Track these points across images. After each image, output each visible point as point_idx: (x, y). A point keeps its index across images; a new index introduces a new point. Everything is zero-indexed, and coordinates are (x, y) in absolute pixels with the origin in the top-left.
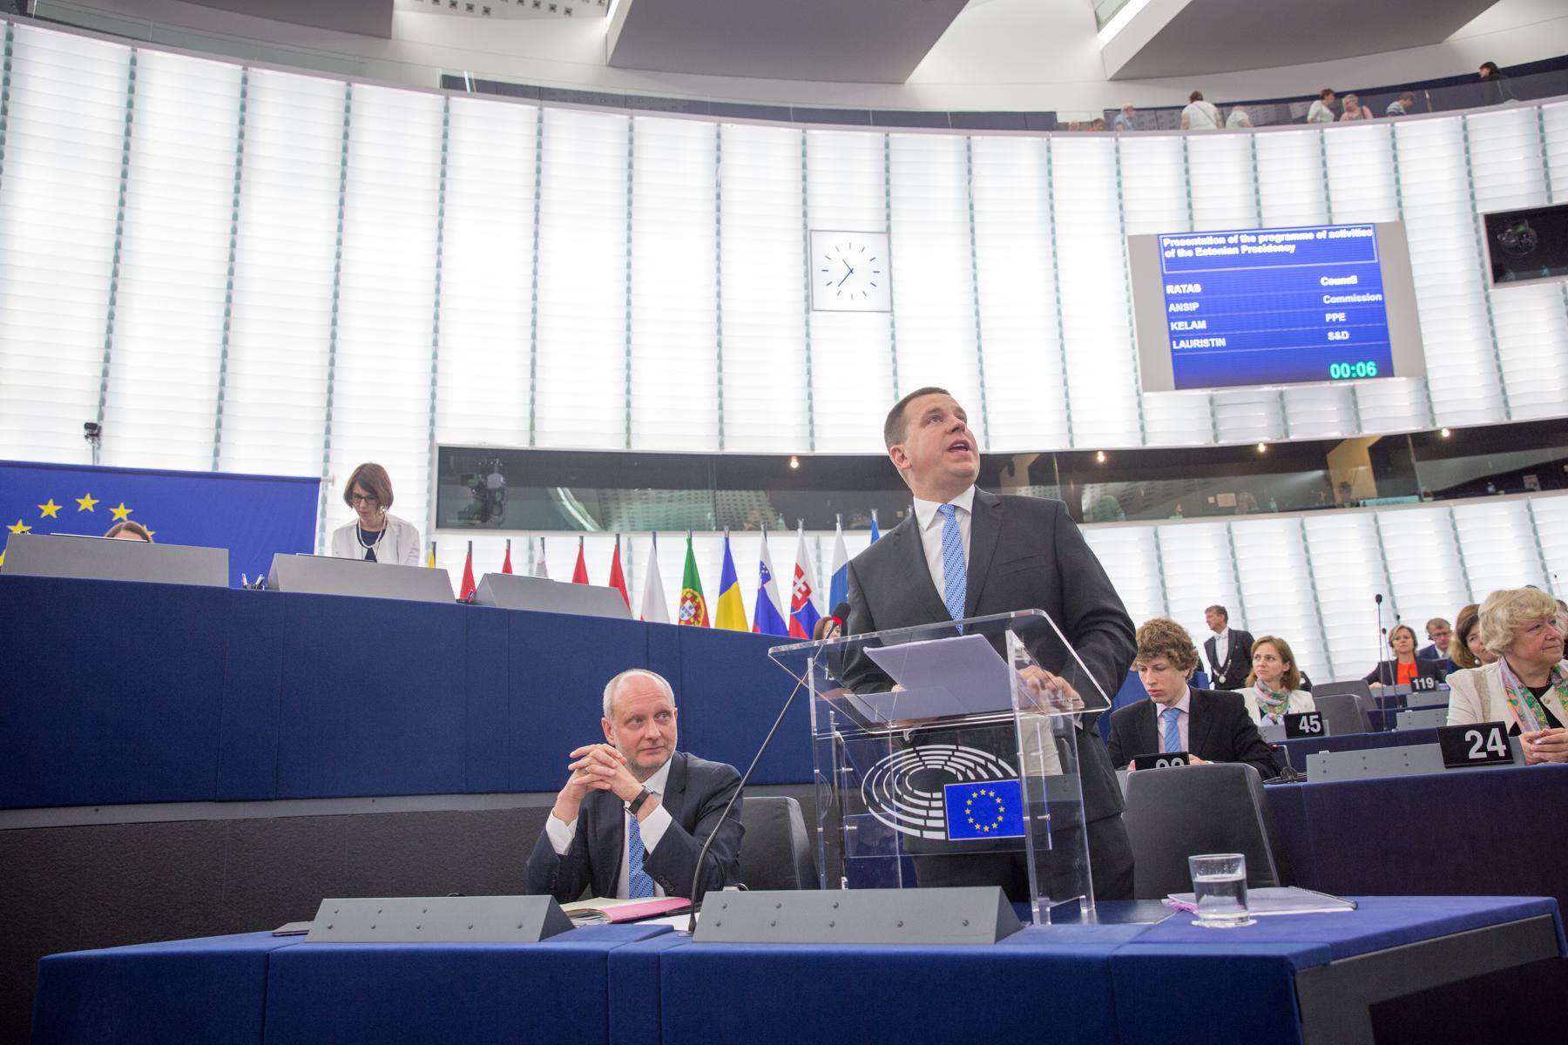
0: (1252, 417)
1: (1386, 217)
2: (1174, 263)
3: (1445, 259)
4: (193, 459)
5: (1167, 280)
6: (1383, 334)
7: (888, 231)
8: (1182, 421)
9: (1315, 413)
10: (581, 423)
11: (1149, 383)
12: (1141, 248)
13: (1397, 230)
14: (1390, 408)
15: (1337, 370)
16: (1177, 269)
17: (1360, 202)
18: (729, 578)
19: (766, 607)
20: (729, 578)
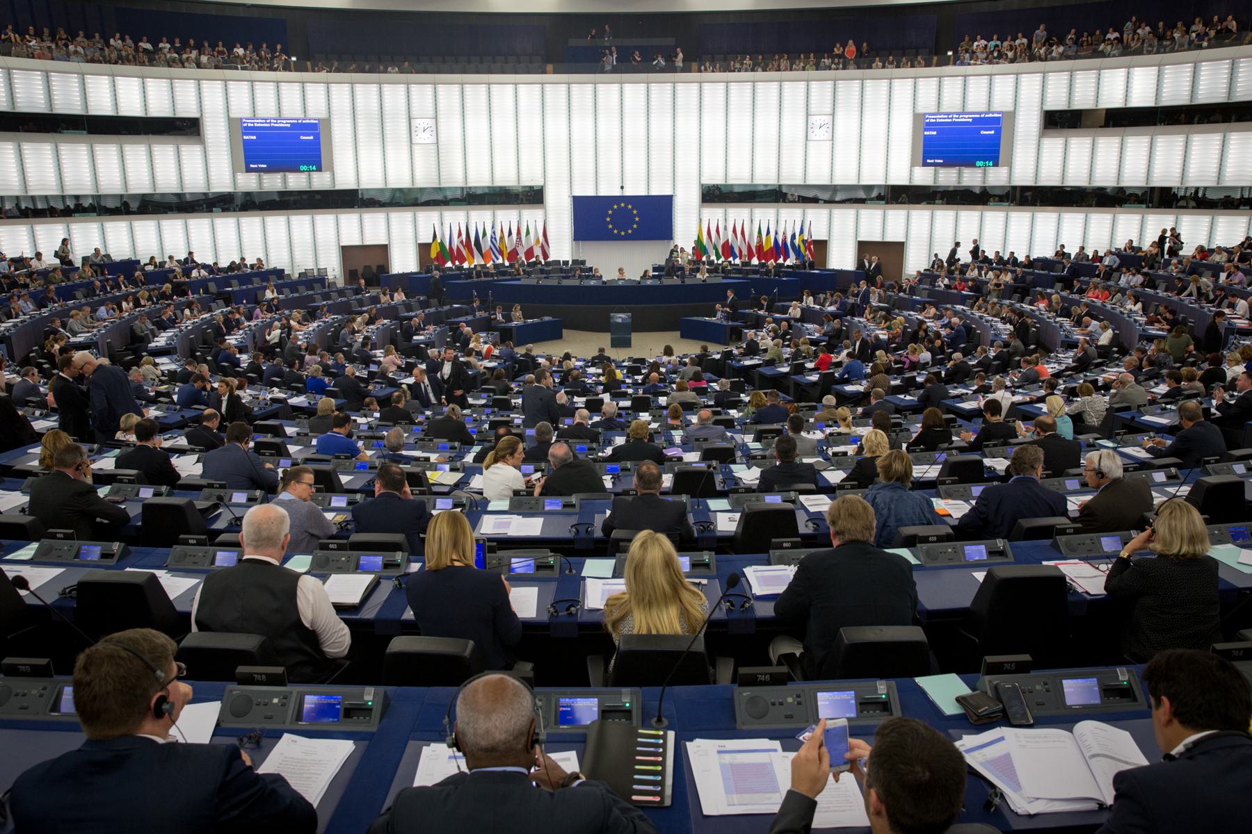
0: (948, 177)
1: (1010, 108)
2: (929, 124)
3: (1028, 122)
4: (643, 193)
5: (926, 130)
6: (998, 152)
7: (833, 115)
8: (923, 177)
9: (971, 178)
10: (739, 176)
11: (913, 165)
12: (918, 118)
13: (1012, 115)
14: (997, 177)
15: (979, 163)
16: (929, 126)
17: (1002, 102)
18: (768, 232)
19: (776, 240)
20: (768, 232)
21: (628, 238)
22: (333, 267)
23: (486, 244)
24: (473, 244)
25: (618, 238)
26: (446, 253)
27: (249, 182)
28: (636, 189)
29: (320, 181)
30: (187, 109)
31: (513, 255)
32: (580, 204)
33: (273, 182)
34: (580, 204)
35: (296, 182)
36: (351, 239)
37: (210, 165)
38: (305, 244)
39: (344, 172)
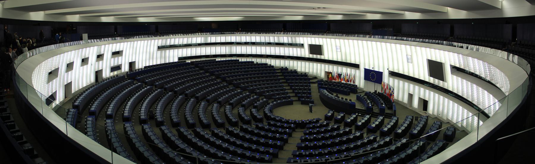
21: (373, 82)
22: (323, 76)
23: (342, 77)
24: (339, 75)
25: (372, 81)
26: (333, 78)
27: (311, 56)
28: (376, 69)
29: (322, 57)
30: (302, 43)
31: (348, 81)
32: (366, 70)
33: (315, 56)
34: (366, 70)
35: (319, 57)
36: (327, 70)
37: (305, 52)
38: (318, 70)
39: (326, 56)
